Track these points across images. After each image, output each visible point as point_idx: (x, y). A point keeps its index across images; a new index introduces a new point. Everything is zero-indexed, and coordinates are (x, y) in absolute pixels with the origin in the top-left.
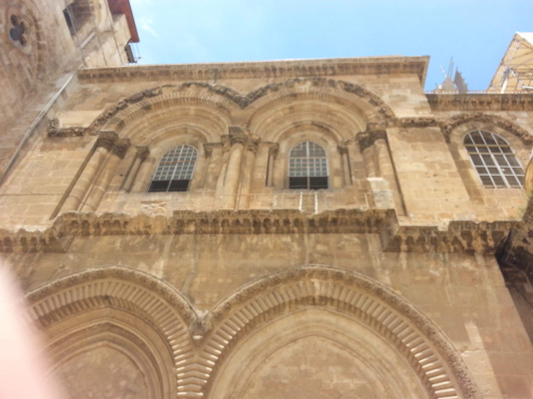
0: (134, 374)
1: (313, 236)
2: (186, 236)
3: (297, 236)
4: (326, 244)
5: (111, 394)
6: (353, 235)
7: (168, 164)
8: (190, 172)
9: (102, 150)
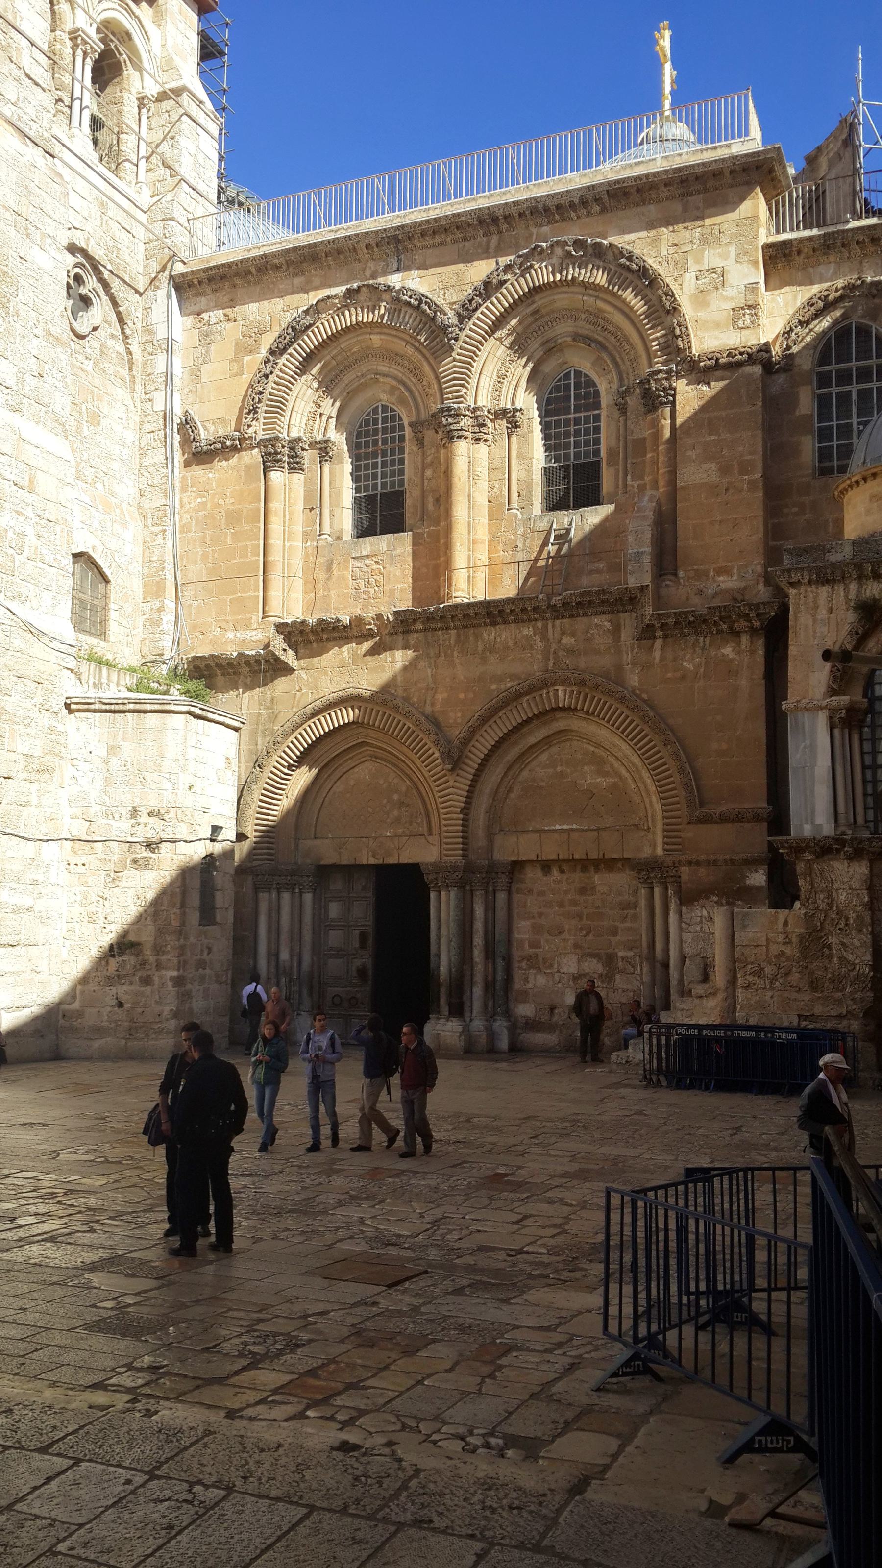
1: (558, 622)
2: (415, 635)
3: (540, 624)
4: (573, 634)
6: (604, 617)
7: (367, 456)
8: (402, 472)
9: (276, 476)
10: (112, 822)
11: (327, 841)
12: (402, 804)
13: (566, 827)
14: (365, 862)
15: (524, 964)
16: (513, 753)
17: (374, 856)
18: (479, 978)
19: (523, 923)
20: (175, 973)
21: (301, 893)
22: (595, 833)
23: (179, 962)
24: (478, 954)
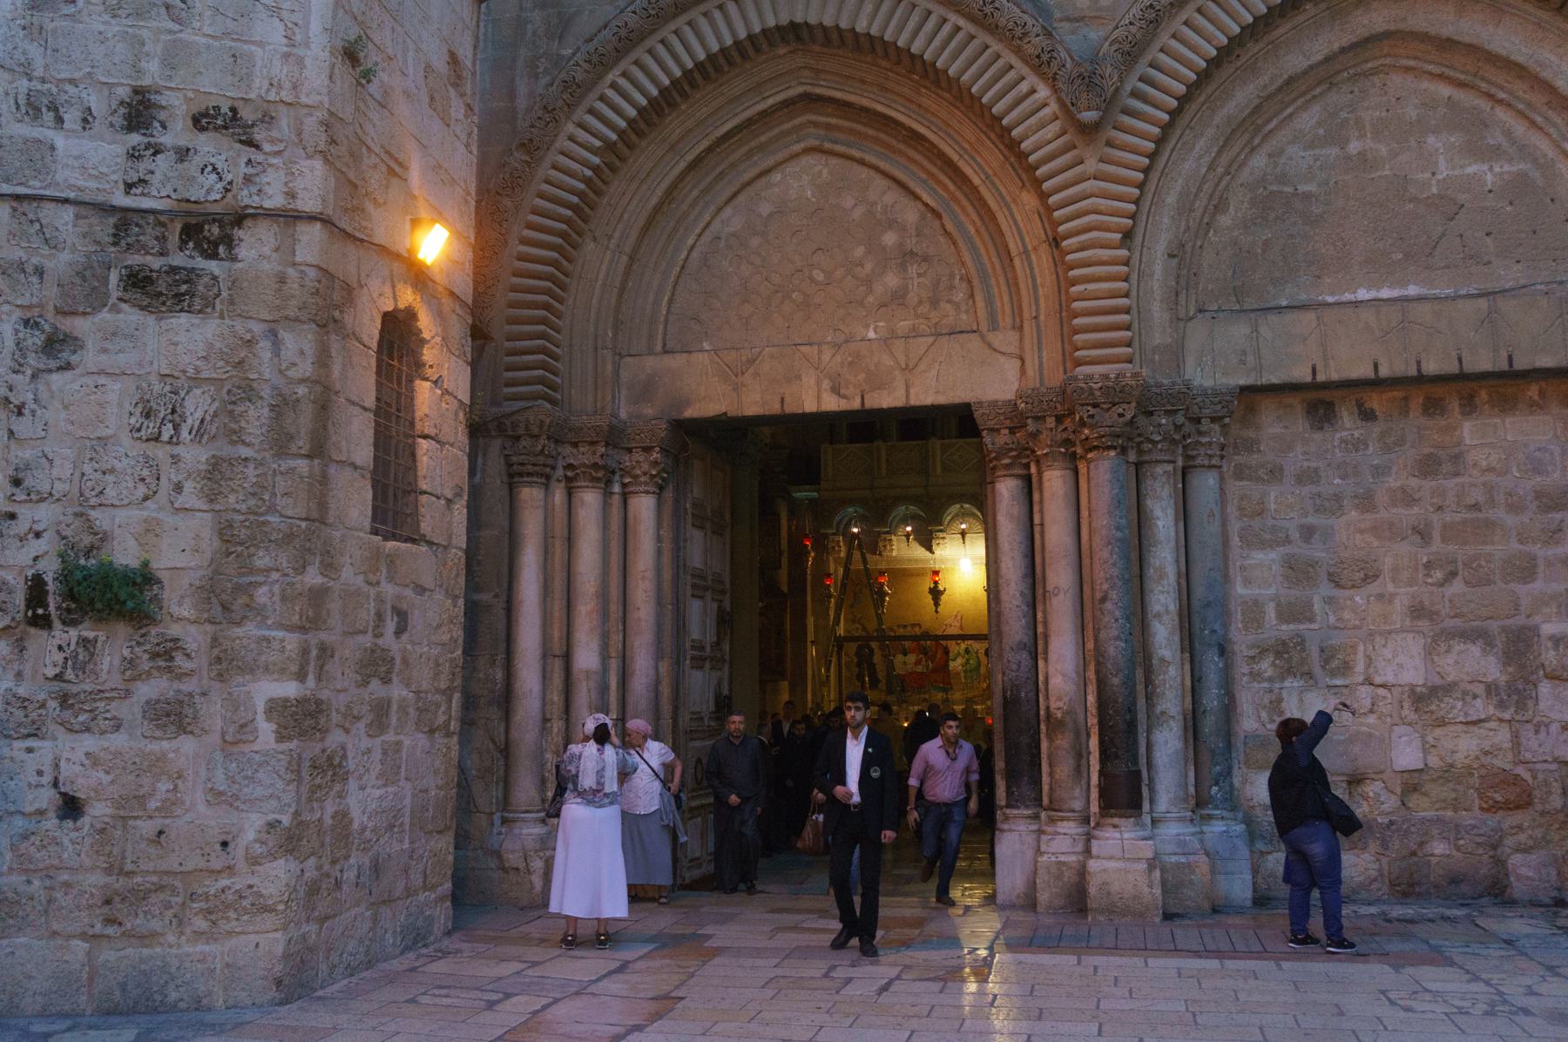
0: (911, 214)
5: (869, 267)
10: (60, 141)
11: (700, 356)
12: (907, 256)
13: (1385, 293)
14: (810, 406)
15: (1266, 666)
16: (1243, 96)
17: (836, 390)
18: (1171, 701)
19: (1258, 556)
20: (290, 689)
21: (625, 498)
22: (1483, 304)
23: (305, 652)
24: (1164, 637)
